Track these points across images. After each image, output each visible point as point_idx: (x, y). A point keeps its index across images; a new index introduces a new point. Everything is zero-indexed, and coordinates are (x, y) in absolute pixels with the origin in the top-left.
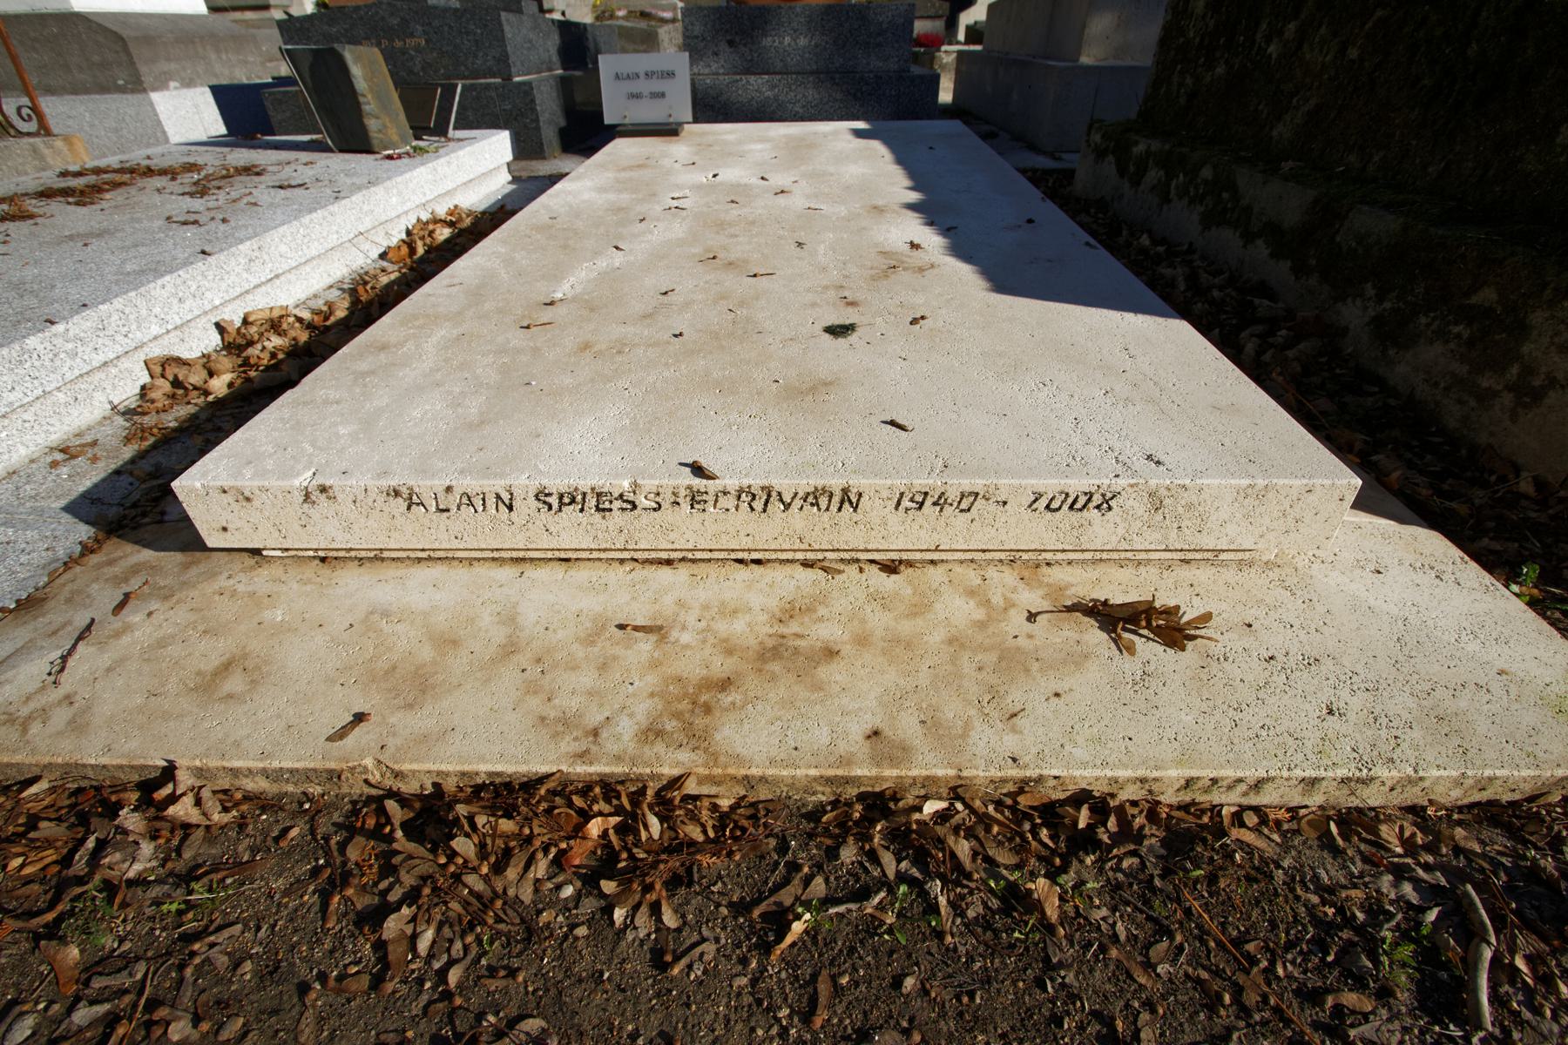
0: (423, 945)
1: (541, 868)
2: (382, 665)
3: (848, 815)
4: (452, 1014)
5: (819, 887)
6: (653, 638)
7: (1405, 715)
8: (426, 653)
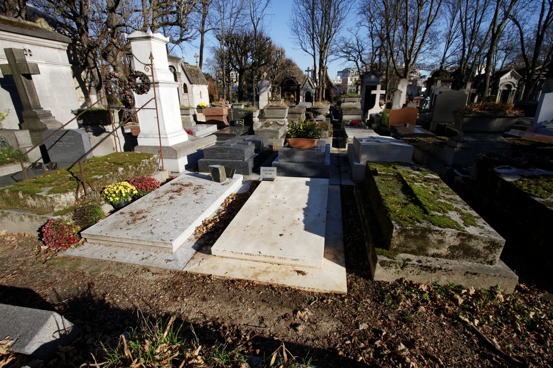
8: (232, 268)
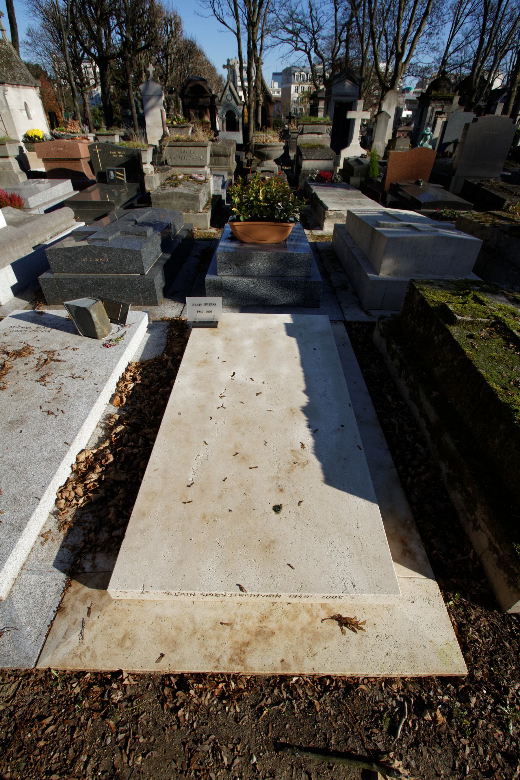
0: (187, 717)
1: (209, 696)
2: (163, 637)
3: (276, 681)
4: (196, 734)
5: (269, 701)
6: (229, 627)
7: (404, 656)
8: (174, 633)
